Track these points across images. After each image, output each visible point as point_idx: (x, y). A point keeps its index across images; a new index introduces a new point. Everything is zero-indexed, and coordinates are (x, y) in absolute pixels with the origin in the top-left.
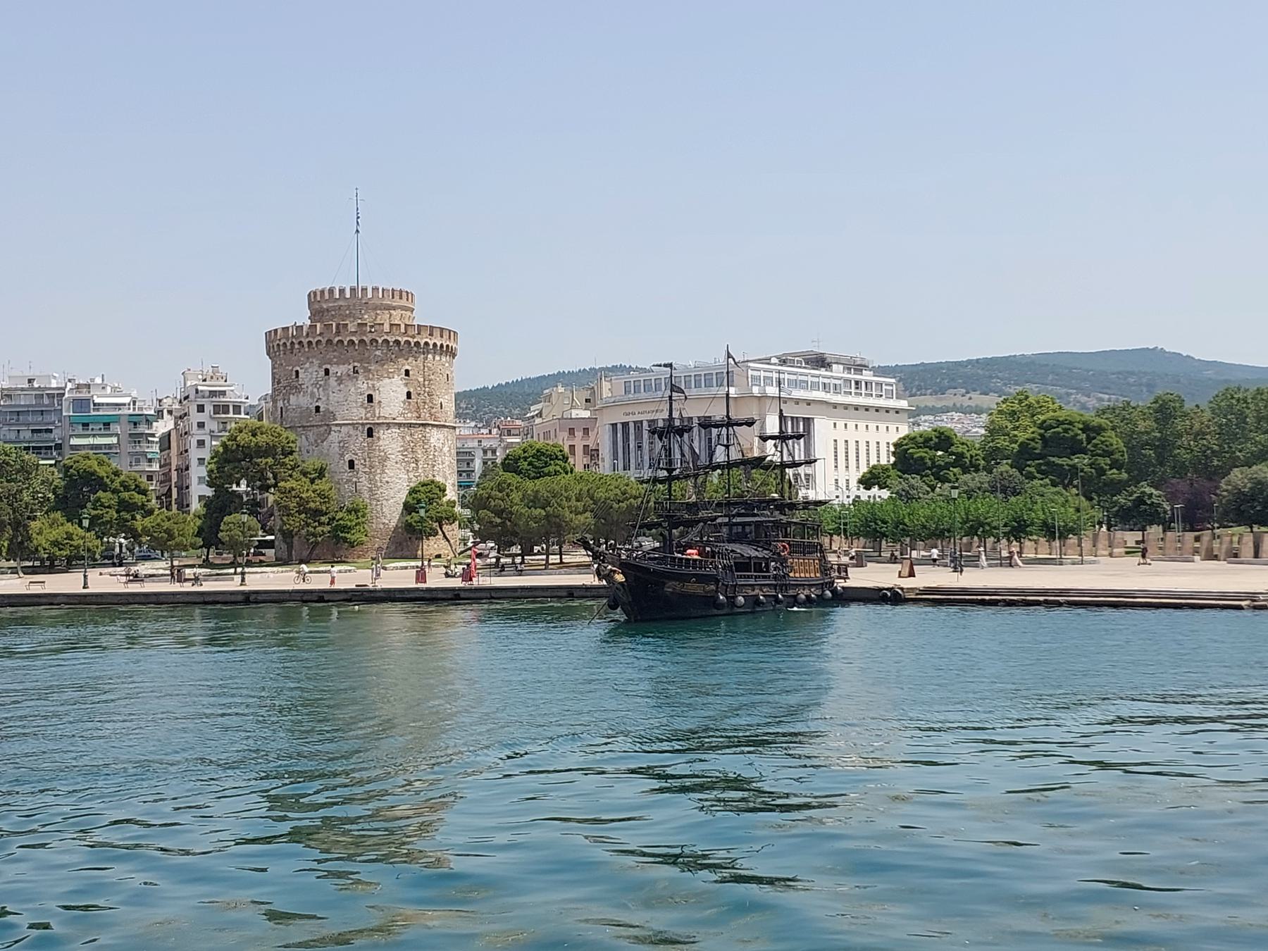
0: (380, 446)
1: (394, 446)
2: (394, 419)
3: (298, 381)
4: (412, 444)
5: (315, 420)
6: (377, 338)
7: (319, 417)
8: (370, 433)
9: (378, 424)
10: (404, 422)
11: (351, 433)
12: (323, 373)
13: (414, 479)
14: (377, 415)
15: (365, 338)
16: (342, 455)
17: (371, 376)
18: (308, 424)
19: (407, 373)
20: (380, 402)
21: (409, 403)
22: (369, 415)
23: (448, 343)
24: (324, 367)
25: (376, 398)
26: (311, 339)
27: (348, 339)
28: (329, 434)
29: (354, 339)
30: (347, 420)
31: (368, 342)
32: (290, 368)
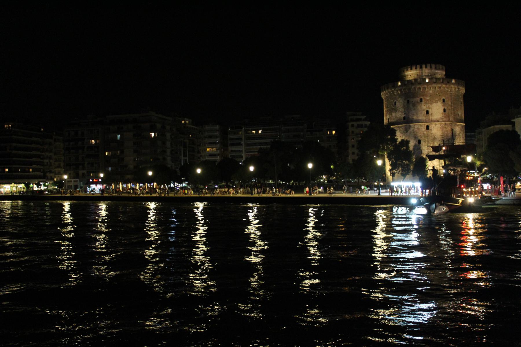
0: (432, 133)
3: (396, 106)
4: (446, 132)
8: (428, 127)
17: (428, 102)
19: (444, 101)
20: (432, 114)
25: (430, 113)
32: (392, 101)
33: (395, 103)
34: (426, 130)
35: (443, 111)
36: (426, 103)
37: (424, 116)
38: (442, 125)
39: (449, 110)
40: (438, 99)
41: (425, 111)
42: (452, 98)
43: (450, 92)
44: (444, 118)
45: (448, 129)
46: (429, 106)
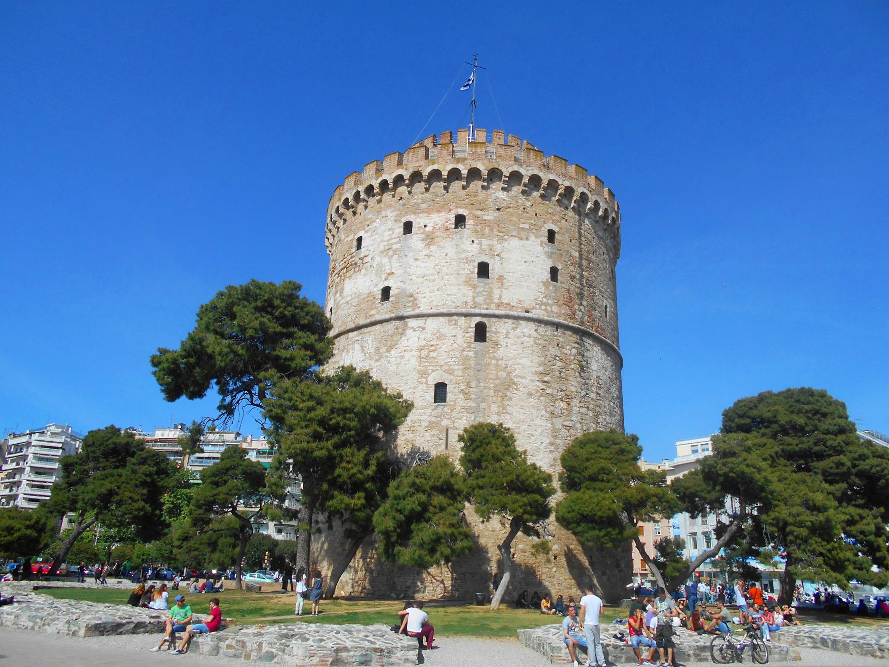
0: (498, 360)
2: (527, 312)
4: (559, 364)
5: (384, 311)
6: (503, 169)
7: (386, 304)
8: (481, 333)
9: (495, 316)
11: (443, 331)
12: (402, 230)
13: (564, 432)
14: (496, 301)
18: (368, 321)
19: (551, 235)
20: (501, 278)
24: (405, 219)
25: (495, 269)
29: (460, 167)
31: (485, 172)
33: (360, 240)
34: (473, 340)
35: (549, 275)
37: (467, 283)
38: (542, 329)
39: (573, 277)
40: (530, 229)
44: (551, 306)
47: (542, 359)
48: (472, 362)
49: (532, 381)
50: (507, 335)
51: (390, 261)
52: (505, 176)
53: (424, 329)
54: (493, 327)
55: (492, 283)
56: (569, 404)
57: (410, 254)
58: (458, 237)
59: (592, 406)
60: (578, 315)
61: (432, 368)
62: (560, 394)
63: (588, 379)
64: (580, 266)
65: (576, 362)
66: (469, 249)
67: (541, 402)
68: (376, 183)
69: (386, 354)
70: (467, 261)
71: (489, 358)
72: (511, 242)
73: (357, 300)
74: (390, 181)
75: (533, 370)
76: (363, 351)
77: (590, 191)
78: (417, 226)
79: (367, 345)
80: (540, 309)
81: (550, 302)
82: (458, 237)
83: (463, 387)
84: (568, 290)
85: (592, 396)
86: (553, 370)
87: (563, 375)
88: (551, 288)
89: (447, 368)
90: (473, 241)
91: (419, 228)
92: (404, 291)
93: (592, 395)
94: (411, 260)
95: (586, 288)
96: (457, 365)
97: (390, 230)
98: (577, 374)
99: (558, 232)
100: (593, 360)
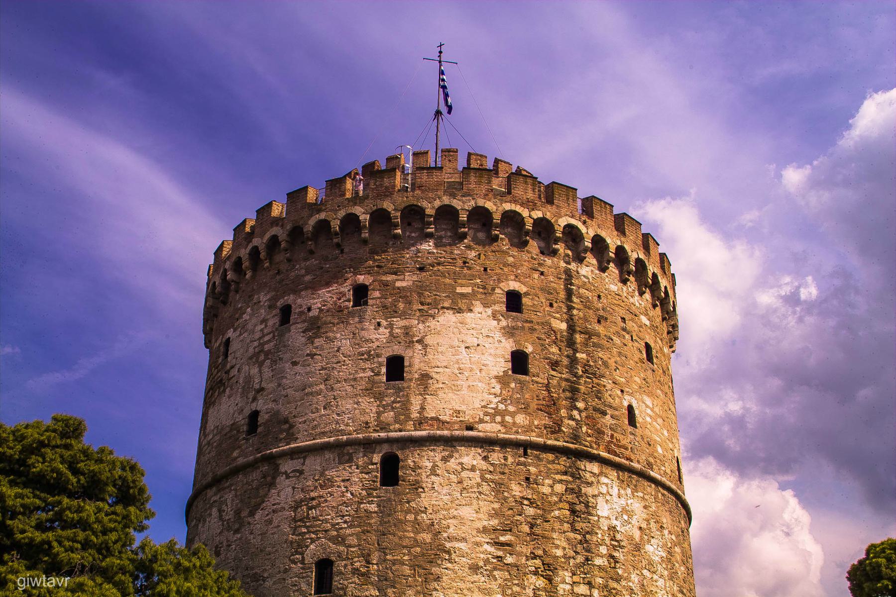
1: (467, 512)
2: (470, 428)
4: (530, 511)
6: (424, 204)
7: (254, 440)
10: (501, 436)
14: (415, 415)
15: (388, 205)
16: (300, 547)
17: (401, 306)
19: (514, 301)
20: (425, 377)
21: (520, 382)
22: (389, 416)
23: (642, 256)
25: (415, 362)
26: (256, 242)
27: (342, 213)
28: (272, 485)
29: (358, 210)
30: (324, 434)
33: (228, 343)
35: (510, 365)
36: (389, 311)
38: (496, 456)
39: (554, 365)
40: (474, 293)
41: (383, 360)
42: (575, 299)
43: (563, 264)
44: (513, 414)
45: (546, 490)
46: (407, 331)
47: (496, 506)
48: (373, 521)
49: (478, 544)
50: (433, 472)
51: (260, 371)
52: (431, 216)
53: (301, 472)
54: (410, 458)
55: (409, 387)
56: (550, 580)
57: (288, 355)
58: (357, 319)
59: (599, 581)
60: (568, 425)
61: (313, 536)
62: (529, 563)
63: (588, 533)
64: (571, 343)
65: (567, 506)
66: (373, 337)
67: (496, 580)
68: (244, 253)
69: (250, 519)
70: (369, 356)
71: (401, 512)
72: (442, 318)
73: (217, 438)
74: (262, 248)
75: (480, 525)
76: (221, 518)
77: (584, 223)
78: (297, 310)
79: (225, 508)
80: (493, 421)
81: (511, 408)
82: (357, 319)
83: (357, 564)
84: (547, 387)
85: (598, 561)
86: (518, 524)
87: (537, 530)
88: (513, 385)
89: (335, 533)
90: (379, 324)
91: (302, 313)
92: (275, 414)
93: (598, 561)
94: (288, 365)
95: (582, 381)
96: (349, 527)
97: (263, 321)
98: (566, 526)
99: (527, 294)
100: (600, 500)
